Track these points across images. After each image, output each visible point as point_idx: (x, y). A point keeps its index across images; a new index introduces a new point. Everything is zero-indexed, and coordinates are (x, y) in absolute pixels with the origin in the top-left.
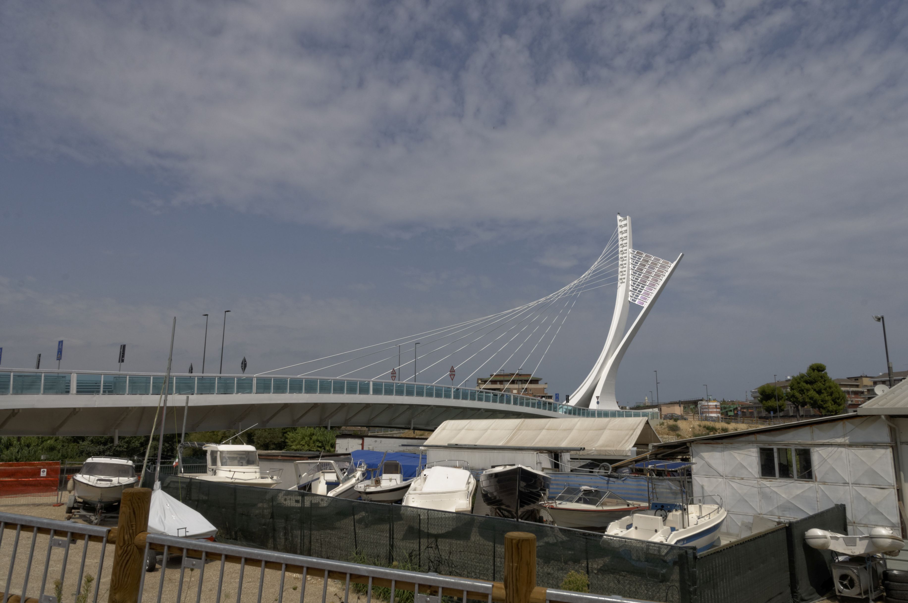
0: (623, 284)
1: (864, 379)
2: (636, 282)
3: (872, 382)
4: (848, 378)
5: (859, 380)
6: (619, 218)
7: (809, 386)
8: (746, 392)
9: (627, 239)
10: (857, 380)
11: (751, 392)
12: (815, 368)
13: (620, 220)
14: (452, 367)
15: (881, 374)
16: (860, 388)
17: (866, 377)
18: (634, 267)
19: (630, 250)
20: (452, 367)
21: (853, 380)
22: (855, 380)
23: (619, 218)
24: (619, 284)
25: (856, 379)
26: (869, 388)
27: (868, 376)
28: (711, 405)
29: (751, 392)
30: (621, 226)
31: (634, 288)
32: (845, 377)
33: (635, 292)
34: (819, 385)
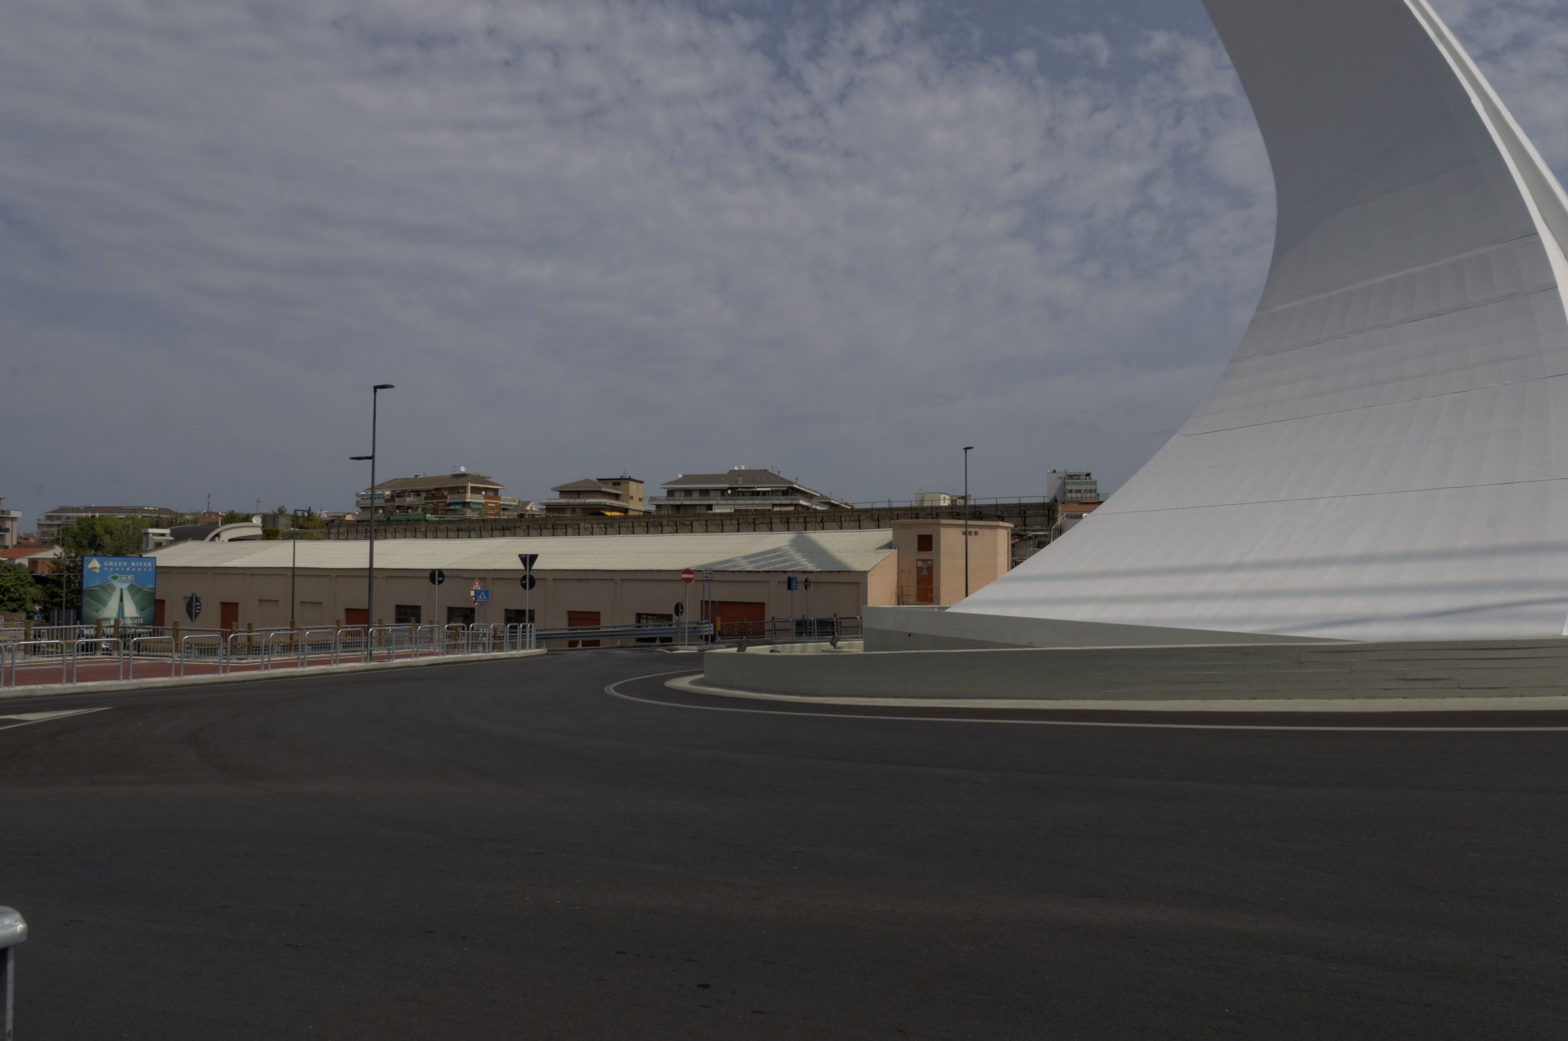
1: (631, 483)
4: (600, 480)
5: (621, 485)
8: (209, 496)
10: (619, 484)
11: (358, 495)
15: (680, 476)
16: (623, 501)
21: (610, 484)
22: (614, 484)
25: (616, 482)
26: (659, 503)
27: (633, 477)
29: (358, 495)
32: (594, 478)
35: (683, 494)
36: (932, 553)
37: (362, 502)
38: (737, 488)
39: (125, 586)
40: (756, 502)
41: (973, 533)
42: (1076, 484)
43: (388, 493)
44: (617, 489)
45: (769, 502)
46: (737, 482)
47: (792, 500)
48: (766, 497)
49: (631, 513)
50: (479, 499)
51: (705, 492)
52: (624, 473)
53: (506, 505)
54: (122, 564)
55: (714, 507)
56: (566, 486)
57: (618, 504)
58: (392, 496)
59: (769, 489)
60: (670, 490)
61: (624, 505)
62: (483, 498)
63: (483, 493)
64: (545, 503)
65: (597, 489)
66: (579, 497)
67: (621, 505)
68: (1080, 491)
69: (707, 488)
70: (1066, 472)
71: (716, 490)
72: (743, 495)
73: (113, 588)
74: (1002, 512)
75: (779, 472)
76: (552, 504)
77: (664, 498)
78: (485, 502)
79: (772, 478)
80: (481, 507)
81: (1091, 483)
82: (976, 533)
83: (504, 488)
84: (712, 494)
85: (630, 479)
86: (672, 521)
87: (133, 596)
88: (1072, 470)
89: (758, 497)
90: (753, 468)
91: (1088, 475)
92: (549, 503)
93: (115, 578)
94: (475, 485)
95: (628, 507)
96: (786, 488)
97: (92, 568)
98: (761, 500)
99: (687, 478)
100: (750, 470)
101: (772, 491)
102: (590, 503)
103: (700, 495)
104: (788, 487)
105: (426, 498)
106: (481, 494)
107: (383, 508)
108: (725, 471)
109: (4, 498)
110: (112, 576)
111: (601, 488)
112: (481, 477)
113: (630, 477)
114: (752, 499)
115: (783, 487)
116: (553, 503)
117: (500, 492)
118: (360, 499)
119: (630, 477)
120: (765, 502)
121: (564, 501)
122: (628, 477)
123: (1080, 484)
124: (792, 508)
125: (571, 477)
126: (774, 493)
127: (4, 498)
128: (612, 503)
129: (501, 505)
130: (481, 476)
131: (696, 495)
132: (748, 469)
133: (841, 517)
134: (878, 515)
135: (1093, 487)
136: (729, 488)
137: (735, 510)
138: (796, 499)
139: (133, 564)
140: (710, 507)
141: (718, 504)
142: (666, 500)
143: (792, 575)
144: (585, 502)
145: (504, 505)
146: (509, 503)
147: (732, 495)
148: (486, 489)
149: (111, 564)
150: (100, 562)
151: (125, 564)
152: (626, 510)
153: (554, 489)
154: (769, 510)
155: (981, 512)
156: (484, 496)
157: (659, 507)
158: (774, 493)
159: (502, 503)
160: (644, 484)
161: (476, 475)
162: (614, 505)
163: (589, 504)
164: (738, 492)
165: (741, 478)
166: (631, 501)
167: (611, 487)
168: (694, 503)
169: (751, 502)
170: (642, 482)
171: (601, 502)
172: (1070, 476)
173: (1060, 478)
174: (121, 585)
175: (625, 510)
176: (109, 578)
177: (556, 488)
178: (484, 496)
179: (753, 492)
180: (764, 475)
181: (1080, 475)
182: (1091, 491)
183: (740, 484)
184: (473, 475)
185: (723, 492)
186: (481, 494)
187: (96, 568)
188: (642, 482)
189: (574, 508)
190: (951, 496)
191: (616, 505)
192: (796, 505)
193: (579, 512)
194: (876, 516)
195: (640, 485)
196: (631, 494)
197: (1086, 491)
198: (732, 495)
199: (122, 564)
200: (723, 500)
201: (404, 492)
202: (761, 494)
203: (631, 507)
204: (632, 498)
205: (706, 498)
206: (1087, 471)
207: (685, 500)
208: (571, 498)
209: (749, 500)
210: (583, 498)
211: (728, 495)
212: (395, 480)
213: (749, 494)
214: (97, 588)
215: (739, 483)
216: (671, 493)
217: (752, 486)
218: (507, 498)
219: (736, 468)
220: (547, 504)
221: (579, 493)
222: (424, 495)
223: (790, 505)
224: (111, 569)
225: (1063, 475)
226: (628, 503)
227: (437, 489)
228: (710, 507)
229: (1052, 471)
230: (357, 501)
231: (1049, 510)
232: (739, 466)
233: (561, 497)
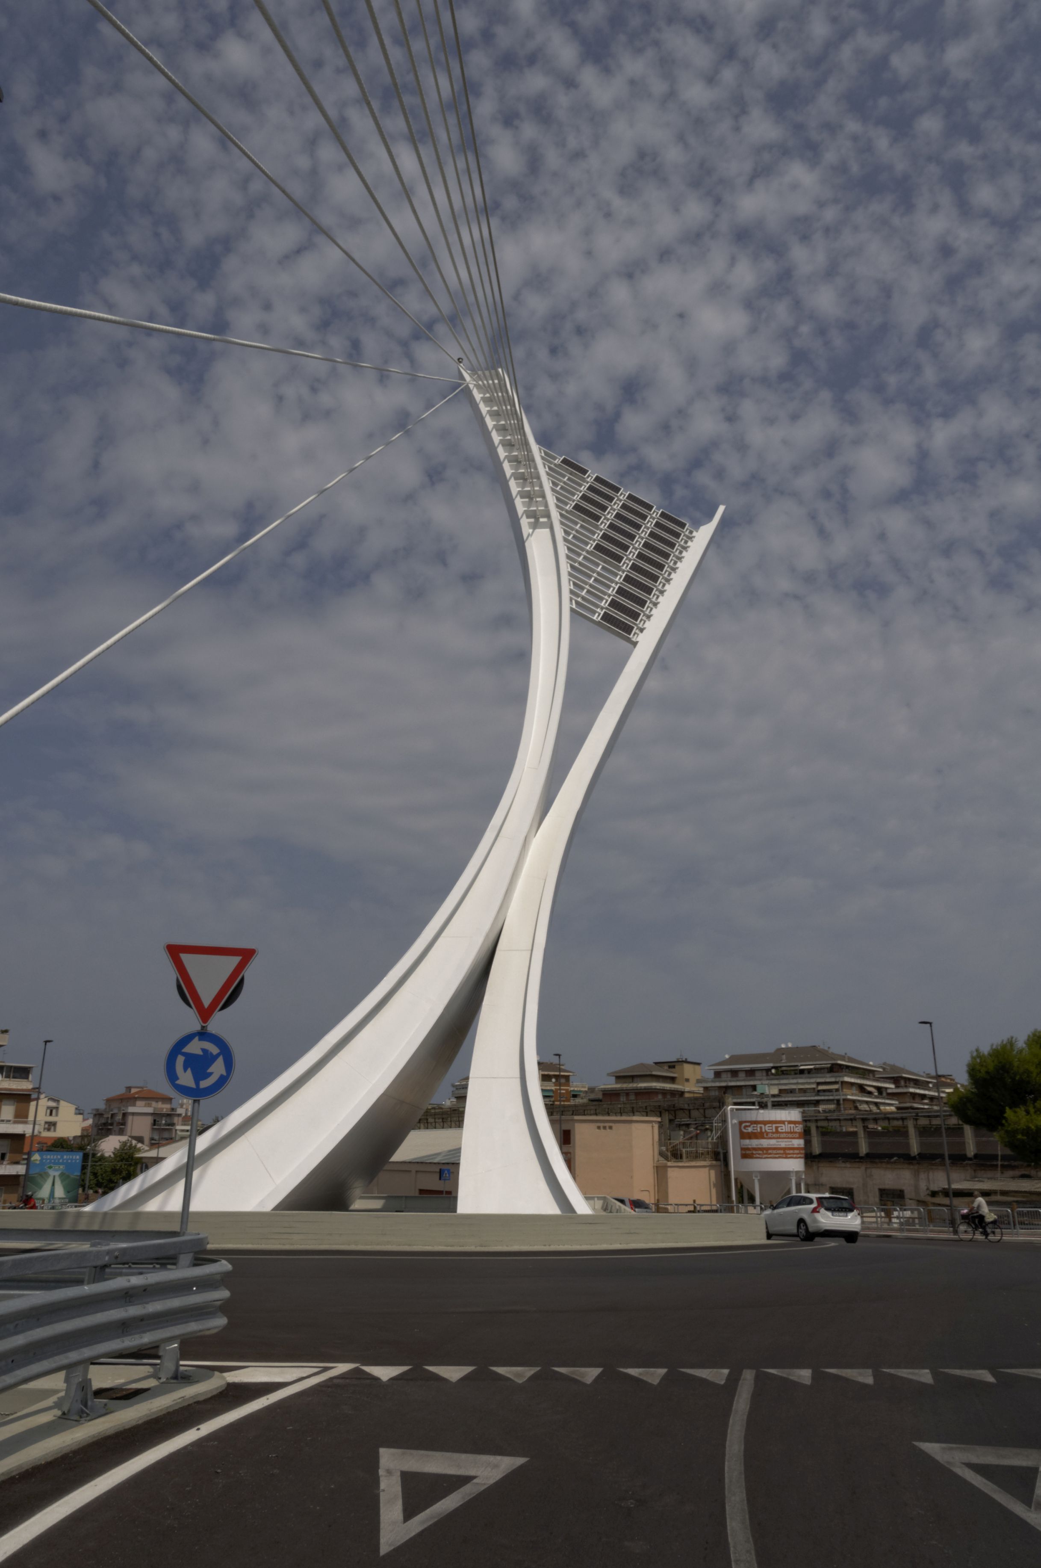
0: (543, 533)
1: (686, 1066)
3: (712, 1072)
4: (656, 1063)
5: (676, 1067)
10: (674, 1067)
11: (453, 1086)
15: (727, 1056)
16: (678, 1084)
17: (686, 1062)
21: (666, 1068)
22: (670, 1067)
24: (526, 530)
25: (672, 1065)
27: (689, 1060)
28: (783, 1122)
29: (453, 1086)
32: (650, 1061)
35: (729, 1074)
36: (571, 1147)
37: (457, 1092)
38: (781, 1067)
39: (57, 1174)
40: (800, 1081)
41: (607, 1128)
44: (672, 1072)
45: (813, 1080)
46: (781, 1060)
47: (836, 1077)
48: (811, 1075)
49: (687, 1095)
50: (550, 1086)
51: (751, 1073)
52: (681, 1055)
53: (576, 1091)
54: (57, 1157)
56: (620, 1071)
57: (670, 1088)
60: (717, 1072)
61: (678, 1088)
62: (553, 1085)
63: (554, 1080)
64: (602, 1088)
65: (648, 1073)
66: (633, 1082)
67: (674, 1088)
69: (751, 1068)
71: (761, 1070)
72: (787, 1074)
73: (48, 1175)
74: (689, 1104)
75: (829, 1048)
76: (607, 1089)
77: (710, 1080)
78: (555, 1089)
79: (817, 1055)
80: (551, 1094)
82: (611, 1128)
83: (575, 1074)
84: (758, 1074)
85: (686, 1062)
86: (439, 1119)
87: (62, 1181)
89: (802, 1076)
90: (800, 1045)
92: (605, 1088)
93: (50, 1168)
94: (546, 1073)
95: (683, 1090)
96: (829, 1065)
97: (34, 1160)
98: (806, 1078)
99: (734, 1059)
100: (797, 1048)
101: (815, 1069)
102: (641, 1087)
103: (746, 1076)
104: (833, 1064)
106: (551, 1081)
108: (771, 1049)
109: (174, 1098)
110: (48, 1166)
111: (652, 1072)
112: (555, 1065)
113: (686, 1059)
114: (796, 1078)
115: (827, 1063)
116: (608, 1088)
117: (571, 1079)
118: (454, 1089)
119: (686, 1059)
120: (809, 1081)
121: (618, 1086)
122: (684, 1059)
125: (626, 1062)
126: (818, 1071)
127: (174, 1098)
128: (663, 1087)
129: (571, 1091)
130: (554, 1063)
131: (742, 1075)
132: (795, 1046)
133: (584, 1111)
134: (608, 1109)
136: (773, 1067)
137: (781, 1091)
138: (840, 1077)
139: (65, 1157)
142: (713, 1081)
143: (444, 1167)
144: (637, 1087)
145: (574, 1091)
146: (579, 1089)
148: (556, 1077)
149: (49, 1157)
150: (40, 1155)
151: (59, 1157)
152: (682, 1093)
153: (609, 1075)
154: (814, 1089)
155: (674, 1105)
156: (554, 1083)
158: (818, 1071)
159: (572, 1089)
160: (701, 1065)
161: (549, 1063)
162: (666, 1088)
164: (782, 1071)
165: (784, 1057)
166: (686, 1084)
167: (667, 1070)
168: (739, 1084)
169: (795, 1081)
170: (699, 1064)
171: (651, 1086)
174: (54, 1173)
175: (680, 1093)
176: (46, 1167)
177: (612, 1073)
178: (554, 1083)
179: (796, 1070)
180: (813, 1051)
183: (784, 1062)
184: (547, 1063)
185: (768, 1070)
186: (551, 1081)
187: (36, 1160)
188: (699, 1064)
189: (627, 1093)
191: (668, 1089)
192: (843, 1083)
194: (607, 1110)
195: (697, 1067)
196: (686, 1076)
199: (57, 1157)
200: (767, 1079)
202: (806, 1072)
203: (687, 1089)
204: (687, 1080)
205: (751, 1078)
207: (730, 1081)
208: (625, 1083)
209: (793, 1078)
210: (637, 1082)
211: (772, 1074)
213: (793, 1073)
214: (36, 1175)
215: (783, 1061)
216: (718, 1074)
217: (796, 1064)
218: (576, 1085)
219: (783, 1046)
220: (603, 1090)
221: (633, 1078)
223: (835, 1083)
224: (48, 1161)
226: (684, 1086)
228: (754, 1088)
230: (453, 1091)
231: (720, 1103)
232: (786, 1044)
233: (617, 1083)
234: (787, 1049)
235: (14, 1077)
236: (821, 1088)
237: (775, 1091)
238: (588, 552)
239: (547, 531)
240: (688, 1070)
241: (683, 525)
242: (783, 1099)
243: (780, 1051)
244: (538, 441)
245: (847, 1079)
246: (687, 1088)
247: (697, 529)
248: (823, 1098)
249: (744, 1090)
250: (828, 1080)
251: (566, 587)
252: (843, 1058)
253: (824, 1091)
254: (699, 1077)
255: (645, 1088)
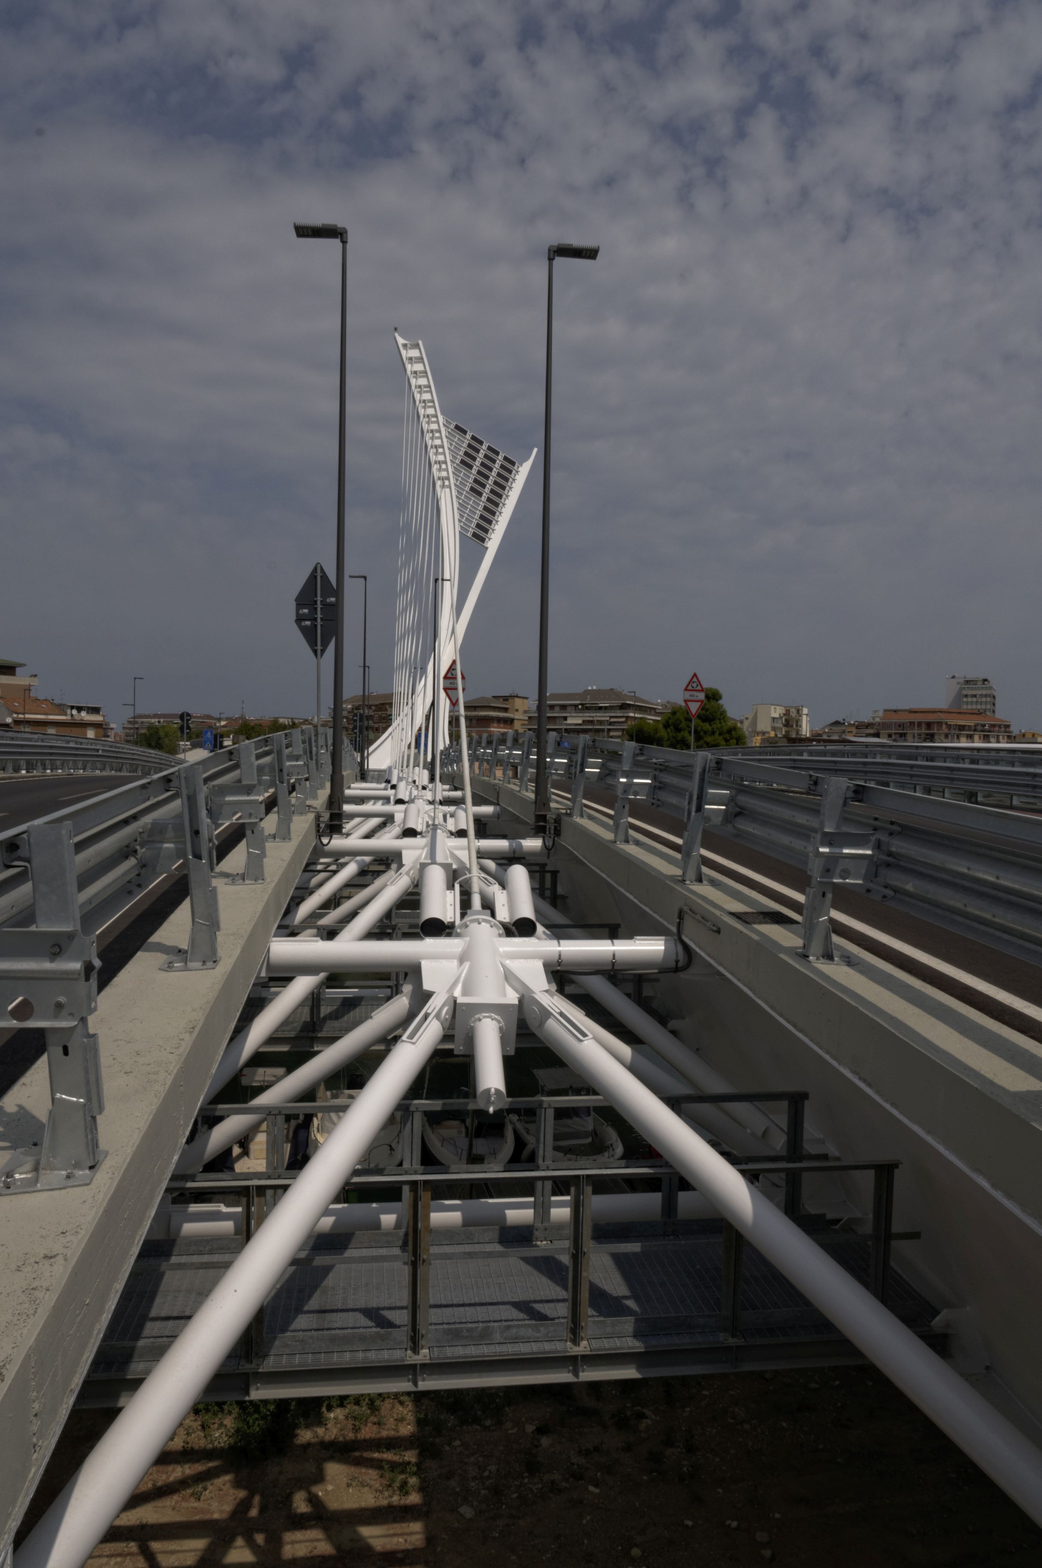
1: (517, 700)
2: (464, 490)
4: (494, 697)
5: (510, 700)
6: (401, 341)
7: (707, 726)
9: (431, 392)
10: (507, 700)
12: (710, 695)
13: (405, 346)
14: (695, 675)
17: (517, 696)
18: (455, 458)
19: (441, 418)
20: (695, 675)
22: (504, 700)
23: (401, 341)
25: (506, 699)
26: (530, 715)
30: (411, 359)
31: (461, 501)
32: (489, 695)
33: (465, 513)
34: (716, 725)
42: (972, 689)
43: (350, 706)
51: (563, 707)
55: (568, 718)
58: (353, 709)
59: (608, 705)
65: (487, 705)
66: (475, 711)
68: (975, 696)
70: (965, 678)
81: (986, 688)
84: (569, 709)
85: (517, 696)
88: (970, 676)
91: (985, 680)
105: (374, 711)
107: (346, 718)
108: (580, 690)
115: (618, 702)
120: (604, 715)
123: (975, 689)
124: (623, 720)
126: (611, 708)
131: (557, 709)
135: (989, 692)
137: (584, 721)
140: (565, 718)
141: (571, 716)
142: (535, 713)
147: (582, 709)
157: (530, 718)
158: (611, 708)
163: (481, 716)
165: (589, 697)
166: (516, 713)
169: (594, 715)
170: (526, 698)
172: (967, 681)
173: (959, 683)
181: (977, 681)
182: (986, 696)
183: (588, 701)
185: (576, 706)
188: (526, 698)
190: (785, 707)
192: (627, 718)
193: (474, 722)
195: (525, 701)
196: (516, 707)
197: (981, 696)
198: (582, 709)
201: (360, 706)
203: (516, 717)
204: (517, 710)
206: (984, 677)
208: (469, 711)
212: (356, 696)
219: (590, 688)
222: (373, 708)
225: (962, 681)
227: (383, 704)
229: (951, 676)
232: (592, 687)
234: (593, 690)
235: (92, 713)
236: (612, 720)
237: (580, 722)
238: (467, 492)
239: (448, 490)
240: (518, 701)
241: (513, 463)
242: (585, 727)
243: (587, 692)
244: (442, 413)
245: (632, 715)
246: (516, 716)
247: (521, 465)
248: (613, 727)
249: (558, 721)
250: (618, 715)
251: (457, 517)
252: (630, 698)
253: (615, 722)
254: (527, 709)
255: (485, 716)
